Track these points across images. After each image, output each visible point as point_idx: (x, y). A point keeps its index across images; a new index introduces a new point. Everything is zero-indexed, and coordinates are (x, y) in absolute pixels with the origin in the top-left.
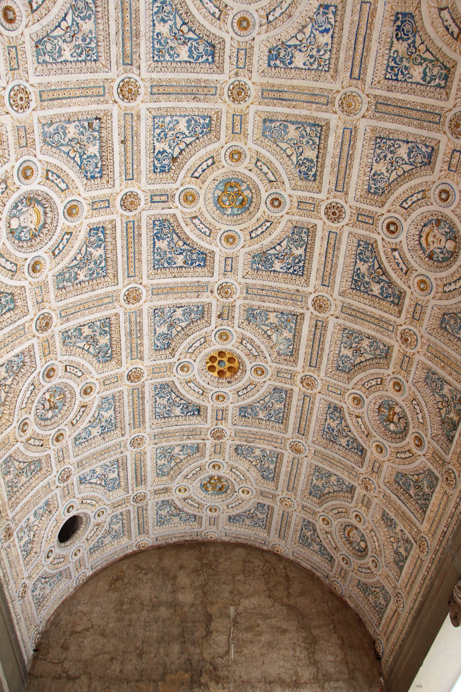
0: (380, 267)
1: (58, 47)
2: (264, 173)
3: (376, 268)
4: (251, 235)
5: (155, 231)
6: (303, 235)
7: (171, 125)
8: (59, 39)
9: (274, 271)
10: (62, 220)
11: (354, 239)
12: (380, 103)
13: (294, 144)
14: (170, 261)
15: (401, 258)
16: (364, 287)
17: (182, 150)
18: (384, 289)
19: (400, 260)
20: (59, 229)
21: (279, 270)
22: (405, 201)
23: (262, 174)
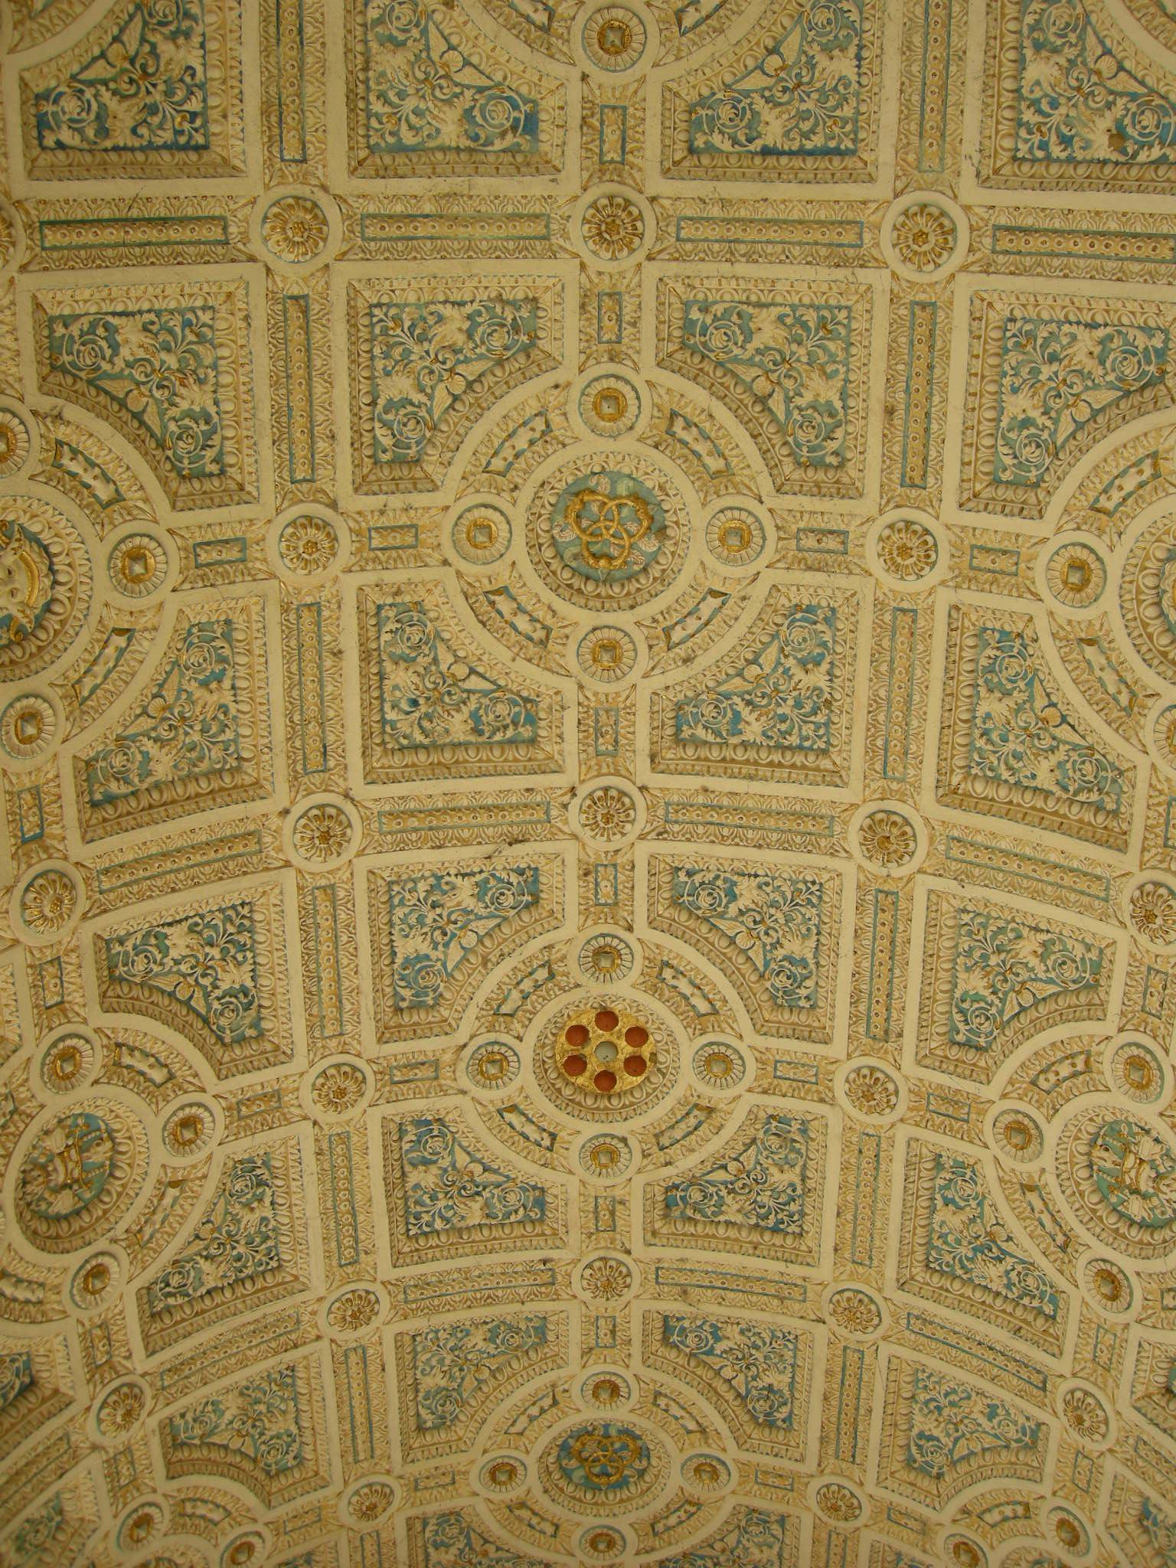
0: (137, 416)
1: (1050, 963)
2: (525, 612)
3: (152, 409)
4: (548, 425)
5: (839, 433)
6: (387, 442)
7: (783, 727)
8: (1041, 975)
9: (461, 304)
10: (1115, 563)
11: (238, 478)
12: (252, 854)
13: (449, 693)
14: (794, 324)
15: (88, 487)
16: (171, 332)
17: (755, 662)
18: (108, 352)
19: (88, 479)
20: (1128, 540)
21: (447, 311)
22: (121, 652)
23: (529, 608)
